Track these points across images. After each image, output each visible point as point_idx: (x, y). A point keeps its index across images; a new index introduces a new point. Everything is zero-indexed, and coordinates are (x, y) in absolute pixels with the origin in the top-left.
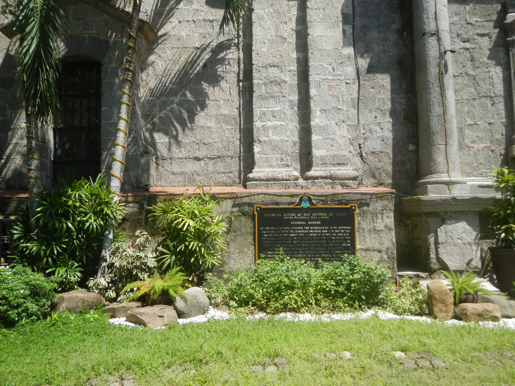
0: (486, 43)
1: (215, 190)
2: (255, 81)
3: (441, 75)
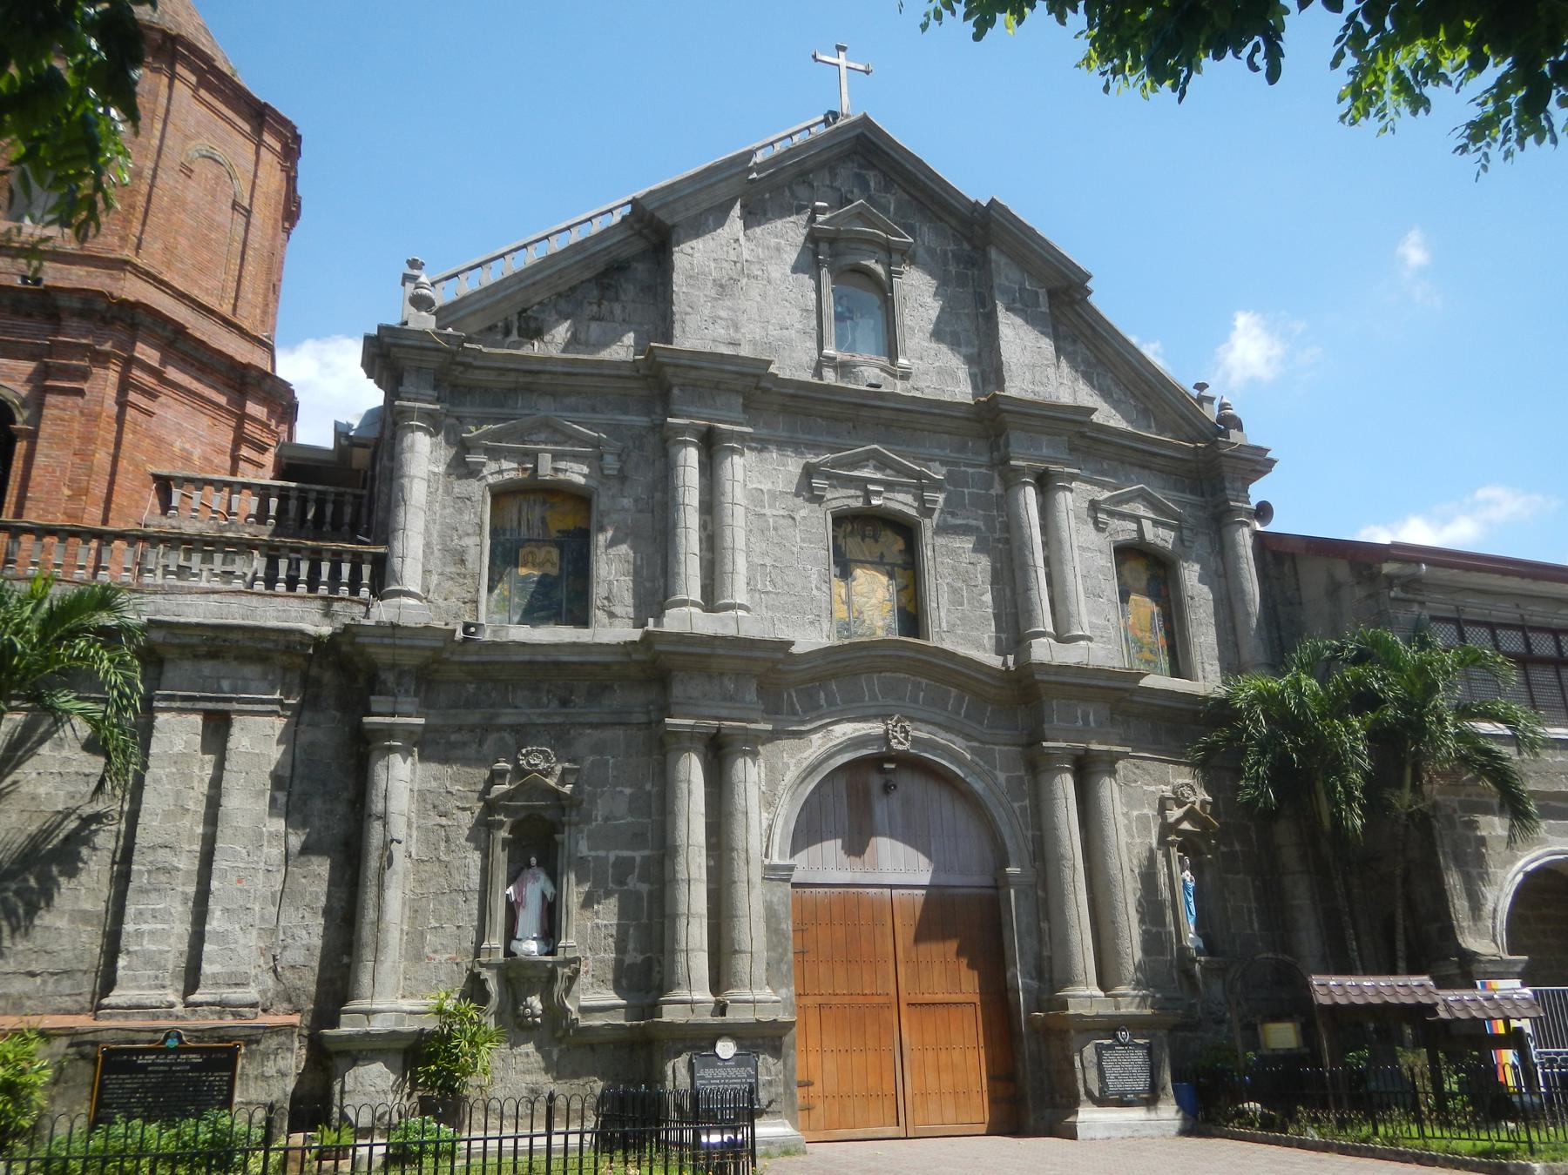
0: (467, 820)
1: (48, 1022)
2: (134, 867)
3: (381, 872)
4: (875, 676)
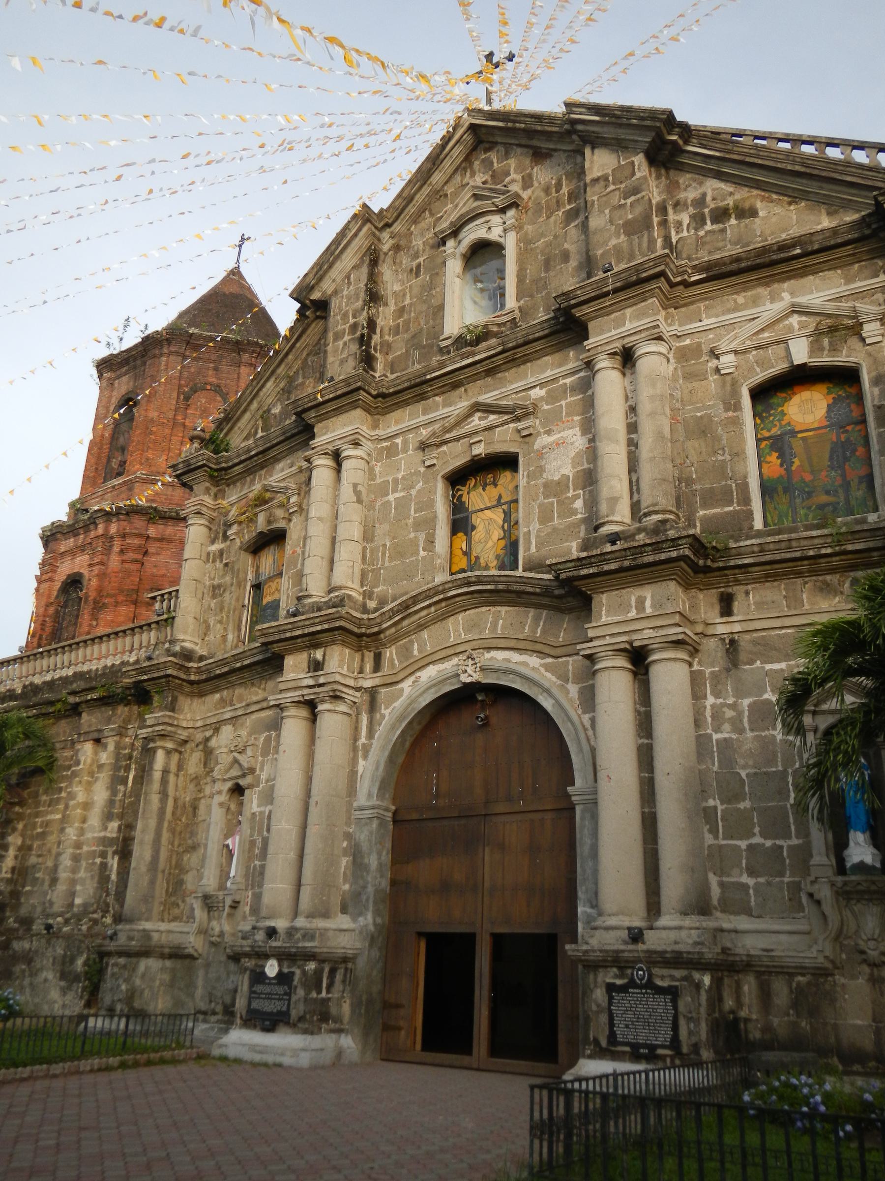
4: (460, 616)
